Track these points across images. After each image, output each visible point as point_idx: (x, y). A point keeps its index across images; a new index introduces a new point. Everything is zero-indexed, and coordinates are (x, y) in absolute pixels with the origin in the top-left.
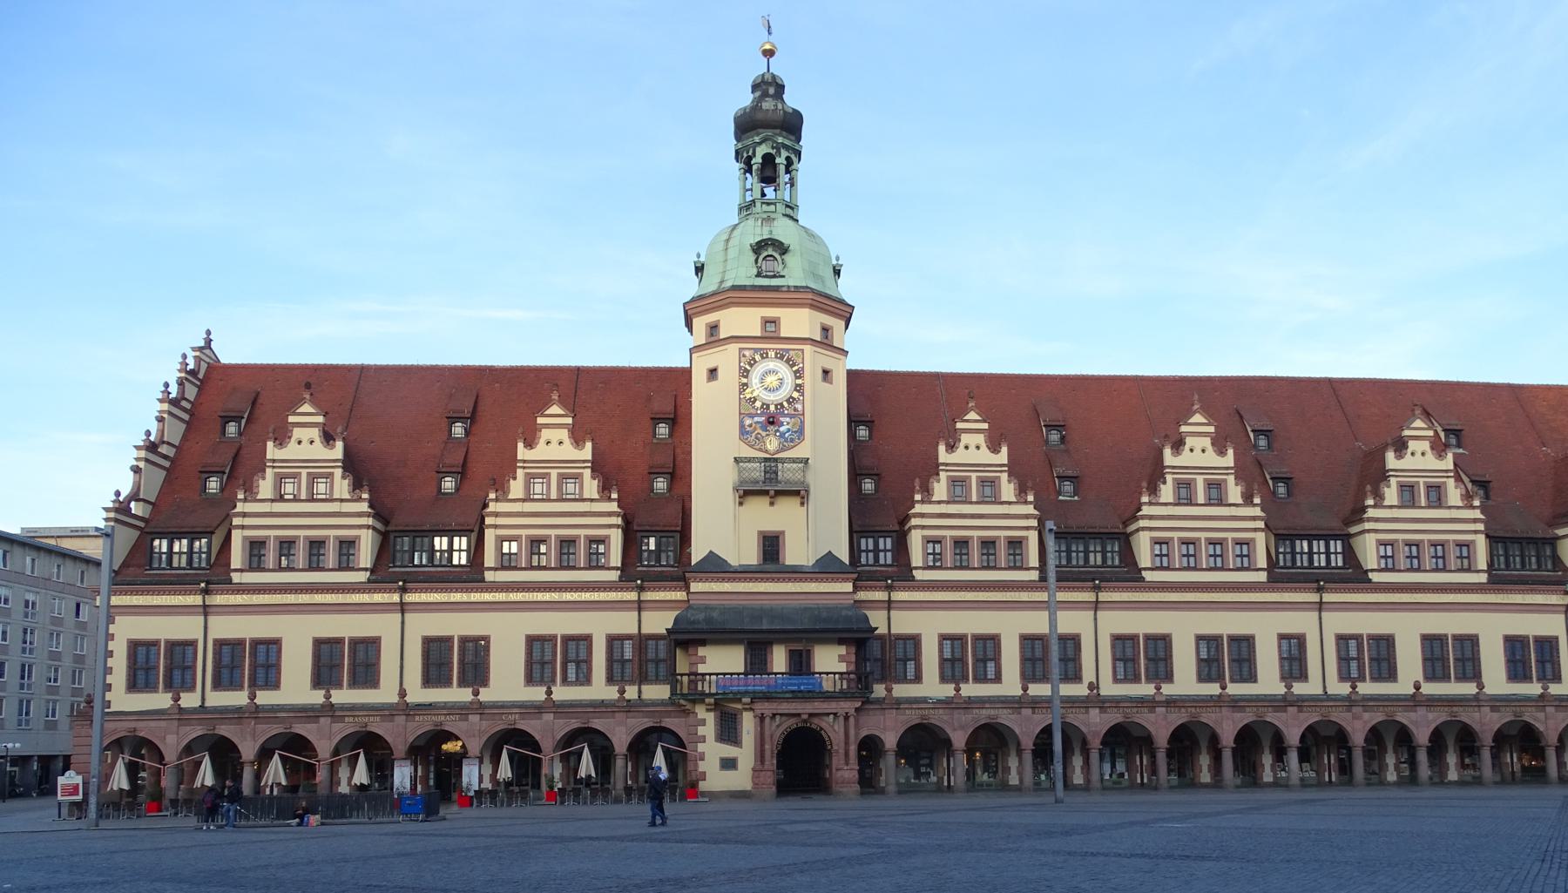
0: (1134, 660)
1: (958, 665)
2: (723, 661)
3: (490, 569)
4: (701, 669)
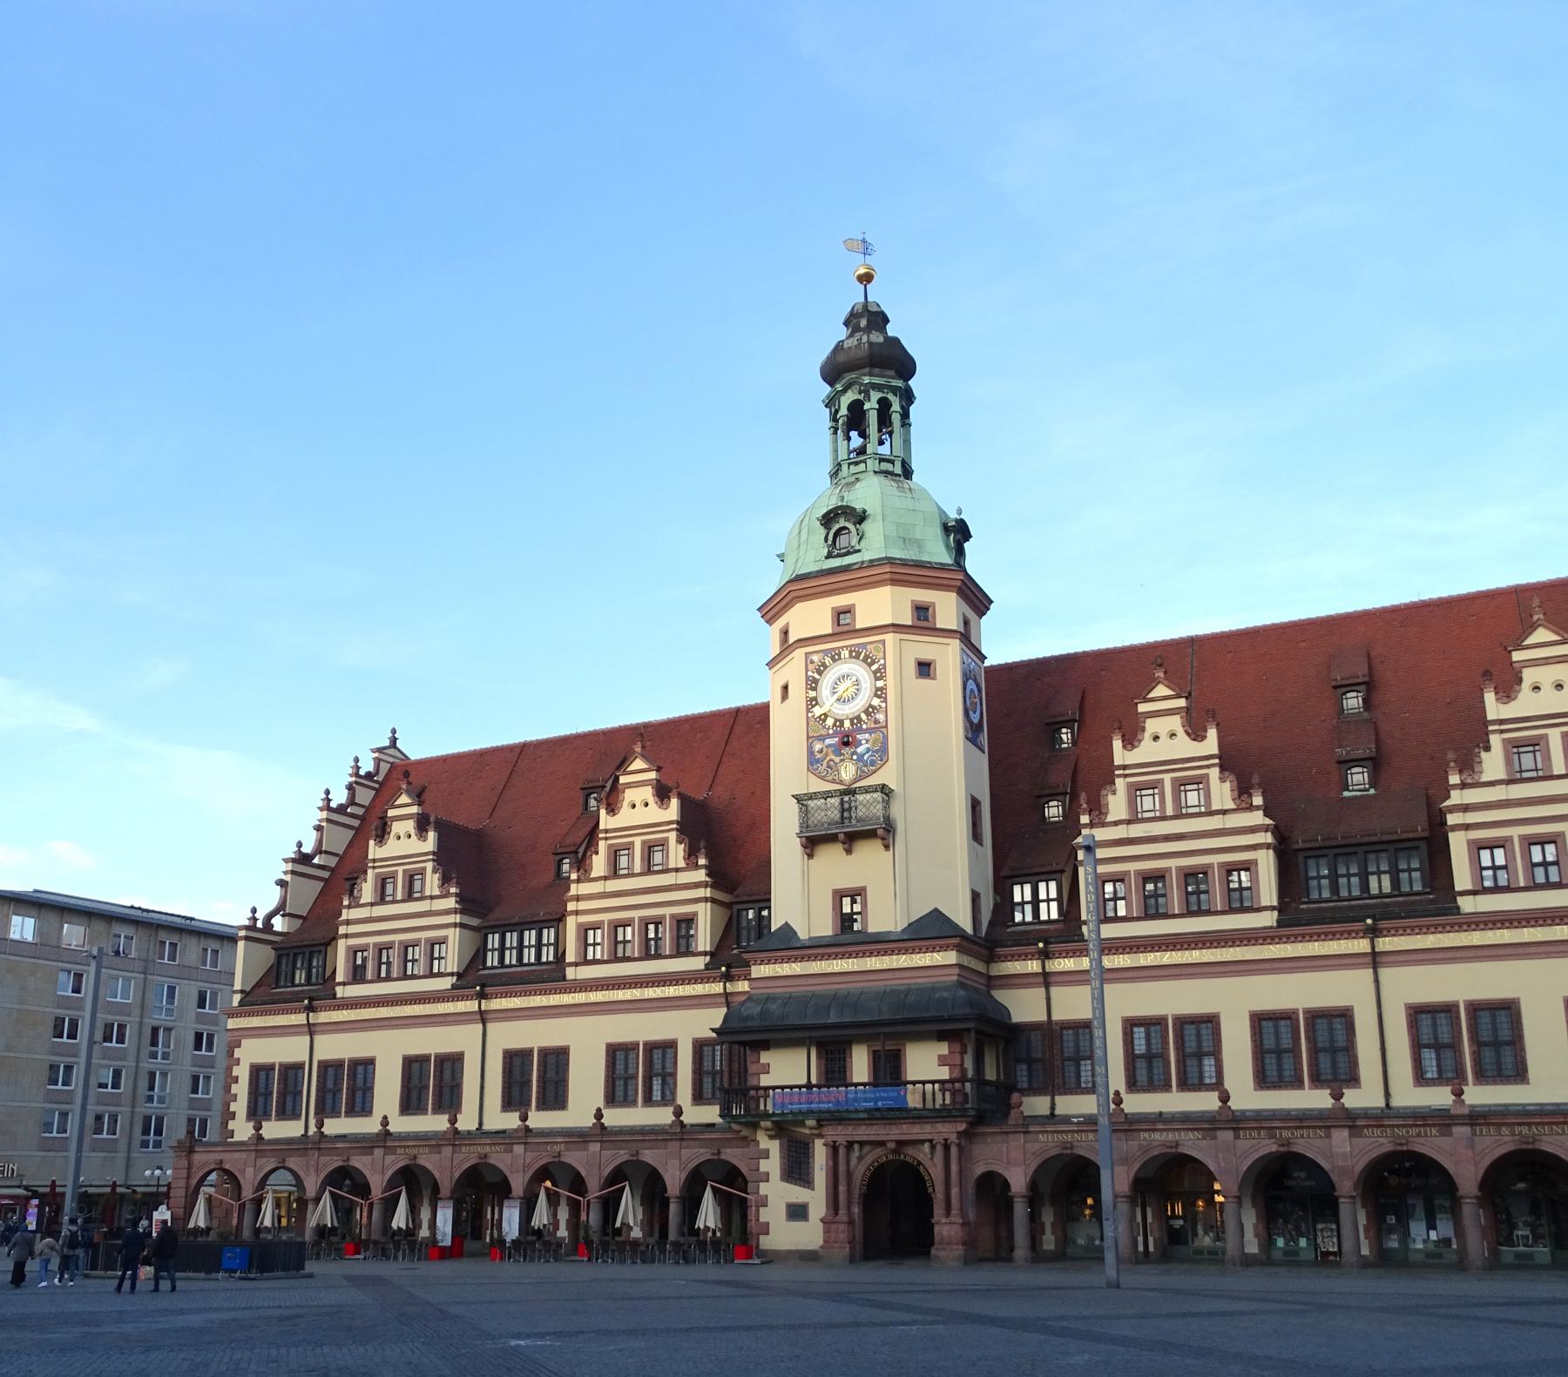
0: (1455, 1046)
1: (1157, 1064)
2: (786, 1069)
3: (571, 964)
4: (765, 1081)
